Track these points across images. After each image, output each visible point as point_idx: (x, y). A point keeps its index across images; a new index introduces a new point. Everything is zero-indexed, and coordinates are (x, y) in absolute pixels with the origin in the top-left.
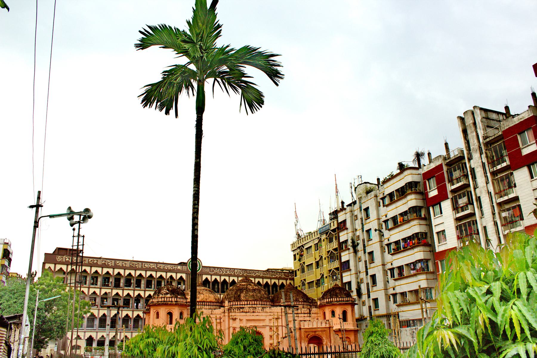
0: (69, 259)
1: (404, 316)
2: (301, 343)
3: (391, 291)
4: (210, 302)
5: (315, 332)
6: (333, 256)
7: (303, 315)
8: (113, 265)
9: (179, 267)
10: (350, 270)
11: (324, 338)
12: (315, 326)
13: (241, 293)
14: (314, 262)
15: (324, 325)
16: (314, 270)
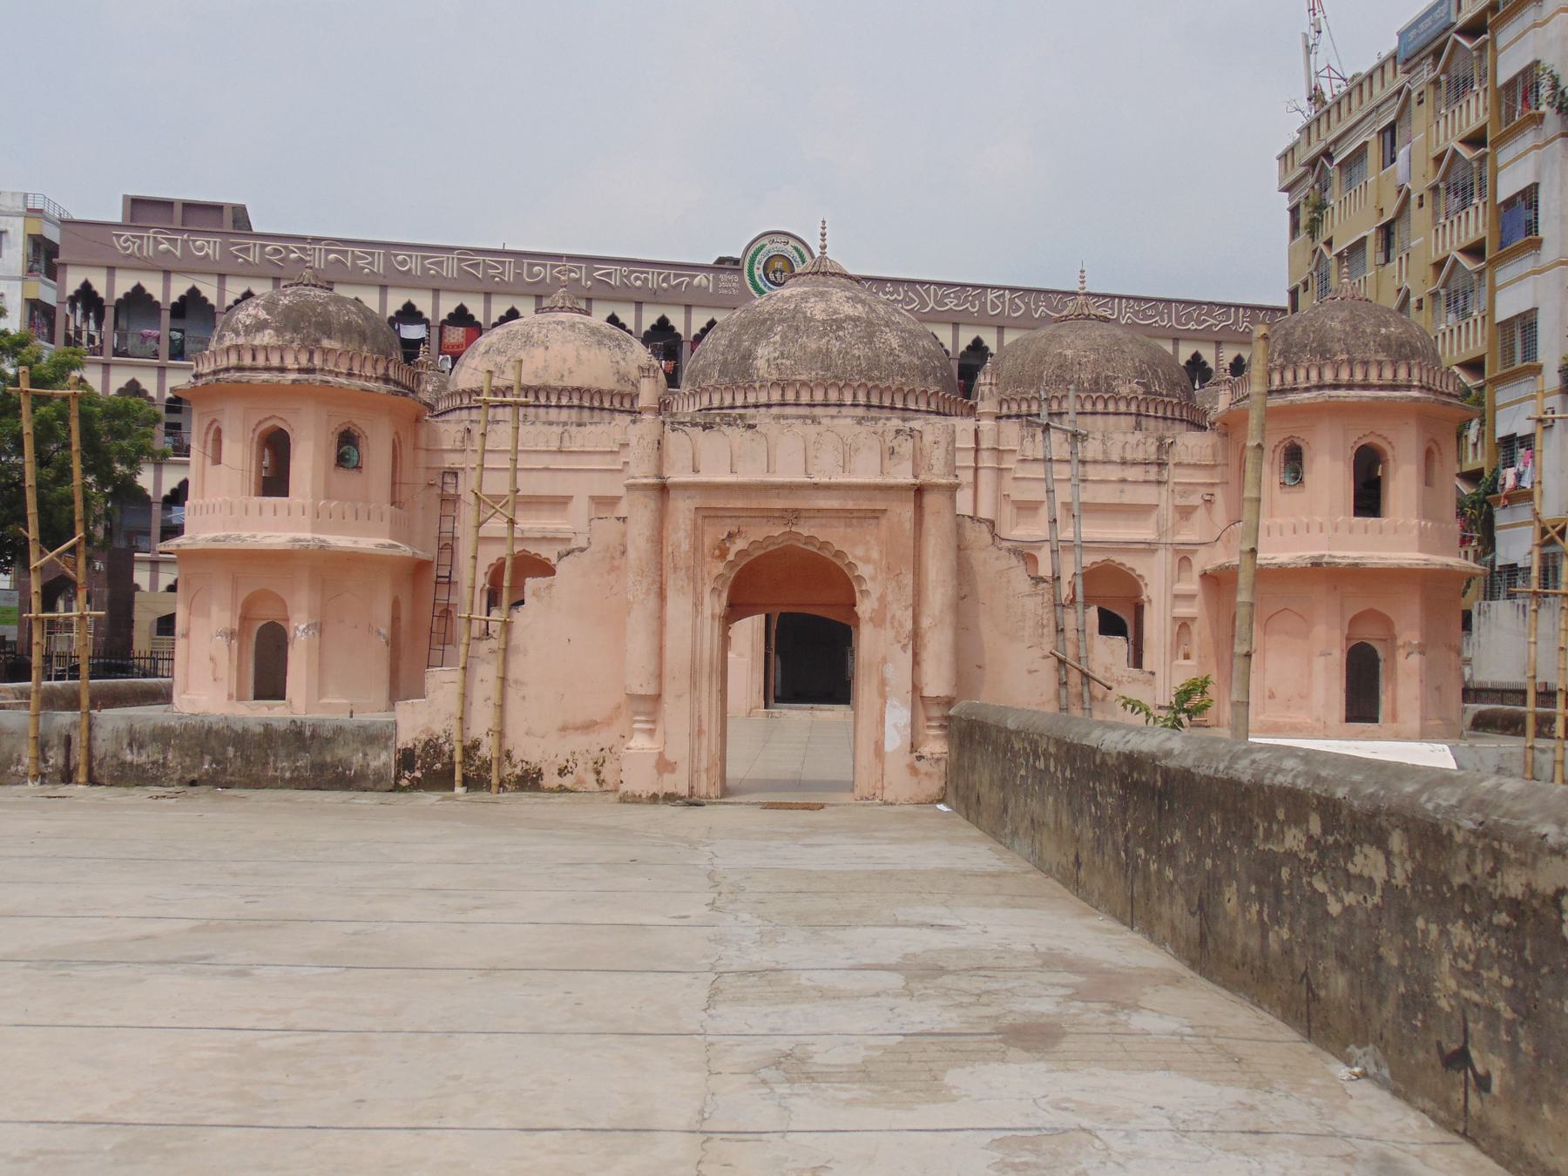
0: (173, 242)
2: (662, 596)
4: (578, 389)
5: (796, 515)
6: (1459, 180)
7: (1114, 473)
8: (380, 267)
9: (700, 279)
11: (864, 570)
14: (1370, 232)
15: (866, 471)
16: (1370, 274)
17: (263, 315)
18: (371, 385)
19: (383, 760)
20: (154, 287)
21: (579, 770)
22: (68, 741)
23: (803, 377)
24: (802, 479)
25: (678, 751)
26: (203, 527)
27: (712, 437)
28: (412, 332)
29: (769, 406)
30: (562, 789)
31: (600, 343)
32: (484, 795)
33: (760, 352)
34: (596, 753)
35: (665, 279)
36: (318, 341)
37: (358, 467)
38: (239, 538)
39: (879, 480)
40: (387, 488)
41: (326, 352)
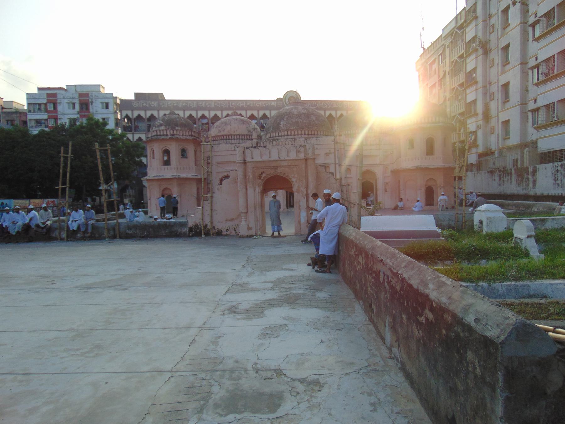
0: (146, 103)
1: (544, 146)
2: (246, 189)
3: (531, 106)
4: (239, 135)
5: (276, 168)
10: (476, 83)
11: (294, 180)
12: (275, 157)
13: (280, 121)
15: (293, 155)
17: (161, 122)
18: (188, 138)
19: (185, 230)
20: (142, 113)
21: (231, 230)
22: (114, 229)
23: (292, 128)
24: (277, 158)
25: (252, 225)
26: (152, 173)
27: (256, 149)
28: (205, 121)
29: (284, 136)
30: (227, 235)
31: (243, 123)
32: (209, 237)
33: (282, 123)
34: (234, 226)
35: (265, 104)
36: (174, 128)
37: (186, 157)
38: (160, 176)
39: (296, 158)
40: (193, 163)
41: (177, 130)
